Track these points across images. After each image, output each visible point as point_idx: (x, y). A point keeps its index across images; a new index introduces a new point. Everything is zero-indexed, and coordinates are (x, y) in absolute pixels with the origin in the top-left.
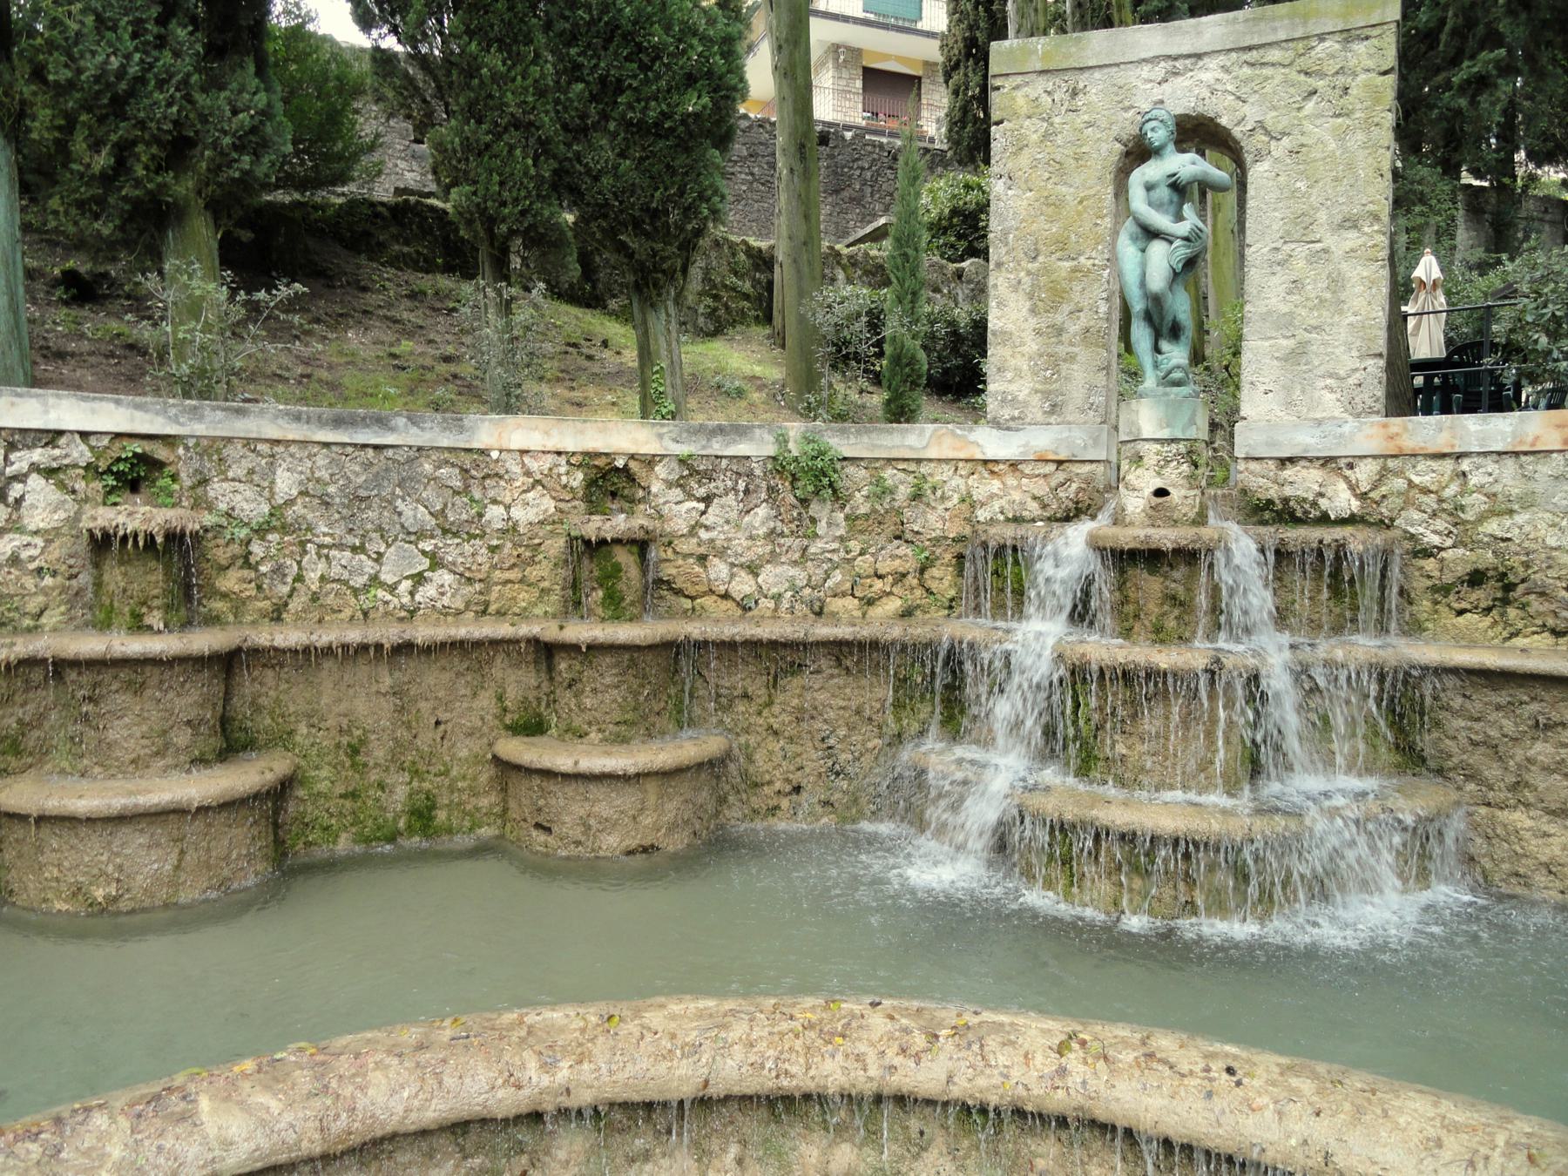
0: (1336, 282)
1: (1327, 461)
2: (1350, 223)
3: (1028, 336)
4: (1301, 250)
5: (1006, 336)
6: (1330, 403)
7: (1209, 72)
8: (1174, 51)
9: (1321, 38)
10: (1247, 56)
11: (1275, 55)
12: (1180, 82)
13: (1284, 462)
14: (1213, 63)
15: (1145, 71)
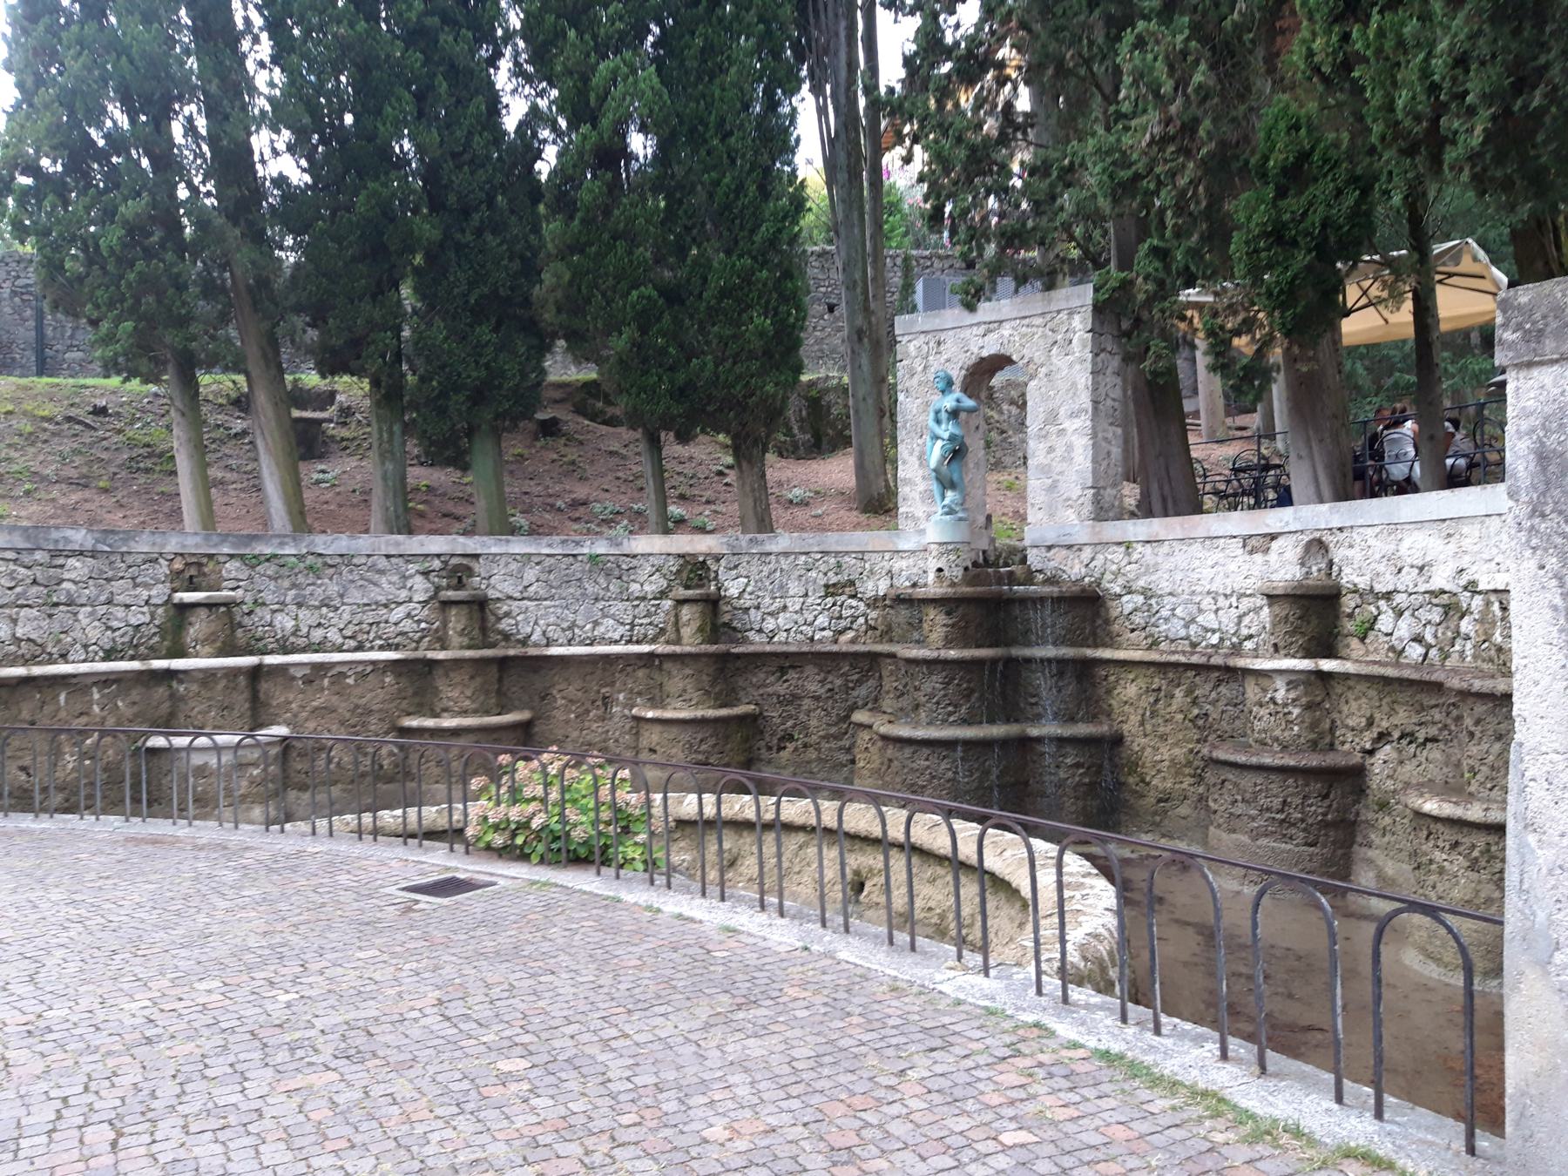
0: (1070, 448)
1: (1070, 547)
2: (1073, 415)
3: (918, 480)
4: (1054, 429)
5: (908, 482)
6: (1071, 516)
7: (1006, 331)
8: (988, 319)
9: (1059, 312)
10: (1026, 321)
11: (1038, 321)
12: (992, 337)
13: (1049, 548)
14: (1007, 325)
15: (975, 330)
